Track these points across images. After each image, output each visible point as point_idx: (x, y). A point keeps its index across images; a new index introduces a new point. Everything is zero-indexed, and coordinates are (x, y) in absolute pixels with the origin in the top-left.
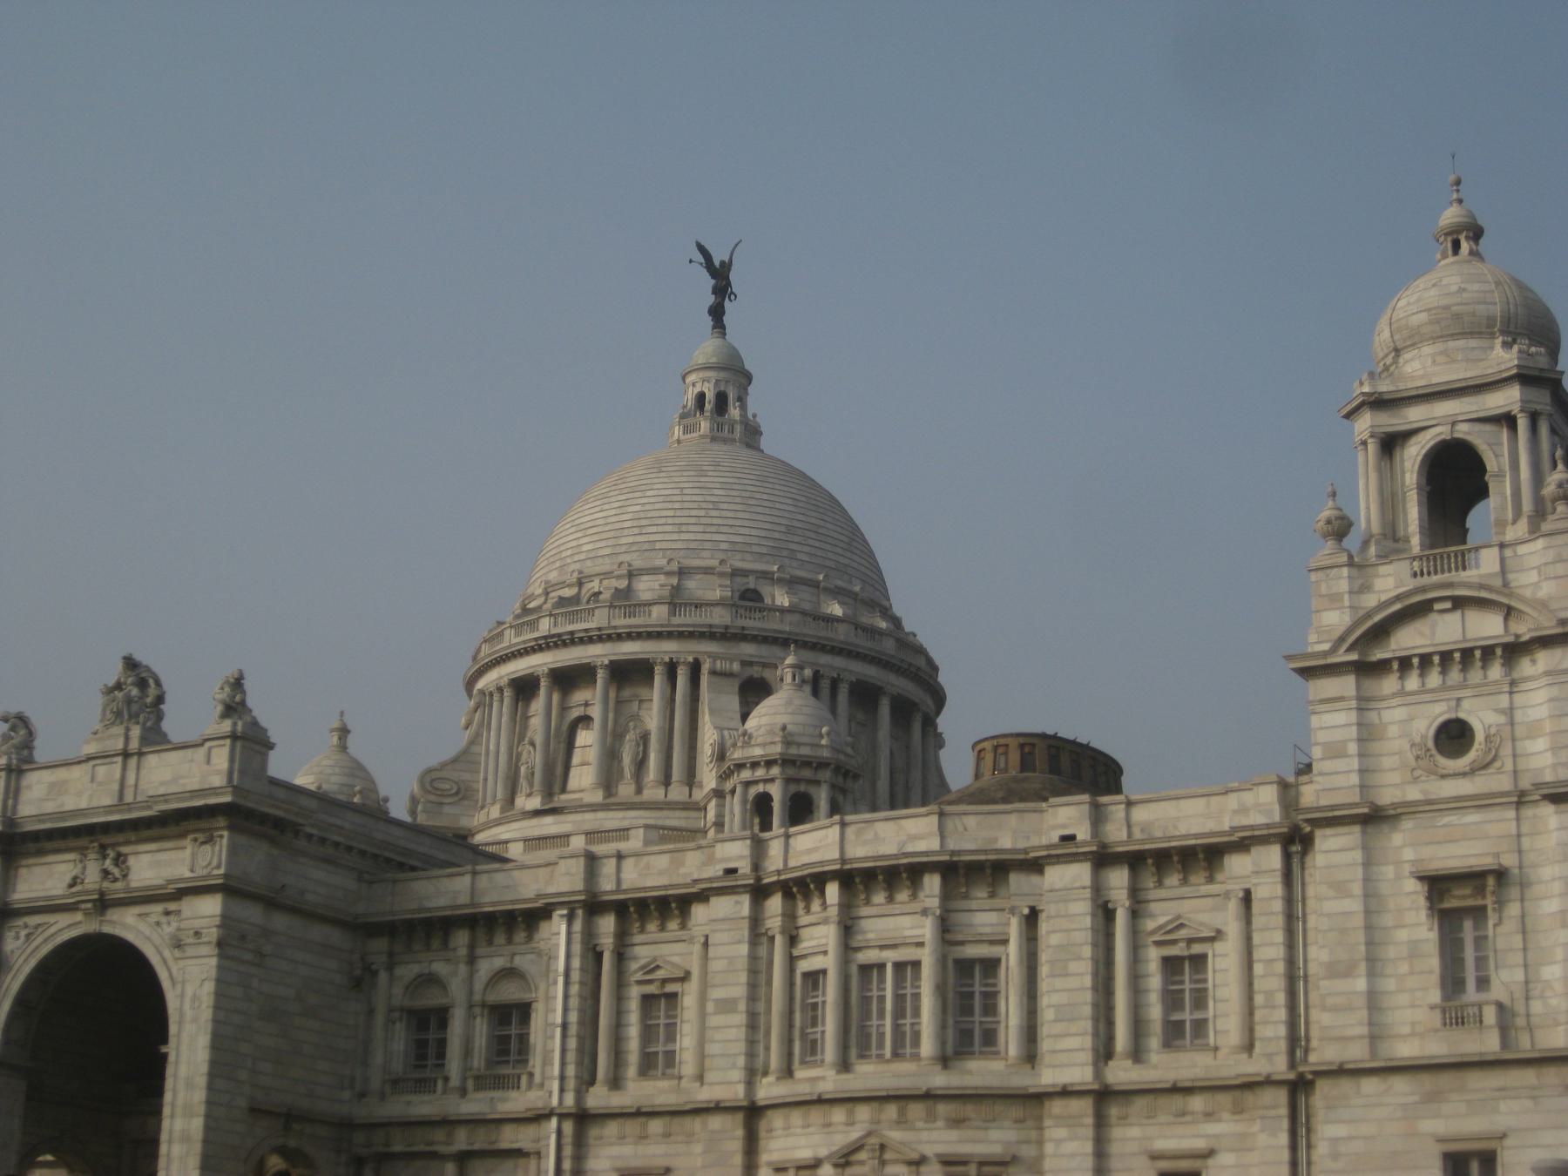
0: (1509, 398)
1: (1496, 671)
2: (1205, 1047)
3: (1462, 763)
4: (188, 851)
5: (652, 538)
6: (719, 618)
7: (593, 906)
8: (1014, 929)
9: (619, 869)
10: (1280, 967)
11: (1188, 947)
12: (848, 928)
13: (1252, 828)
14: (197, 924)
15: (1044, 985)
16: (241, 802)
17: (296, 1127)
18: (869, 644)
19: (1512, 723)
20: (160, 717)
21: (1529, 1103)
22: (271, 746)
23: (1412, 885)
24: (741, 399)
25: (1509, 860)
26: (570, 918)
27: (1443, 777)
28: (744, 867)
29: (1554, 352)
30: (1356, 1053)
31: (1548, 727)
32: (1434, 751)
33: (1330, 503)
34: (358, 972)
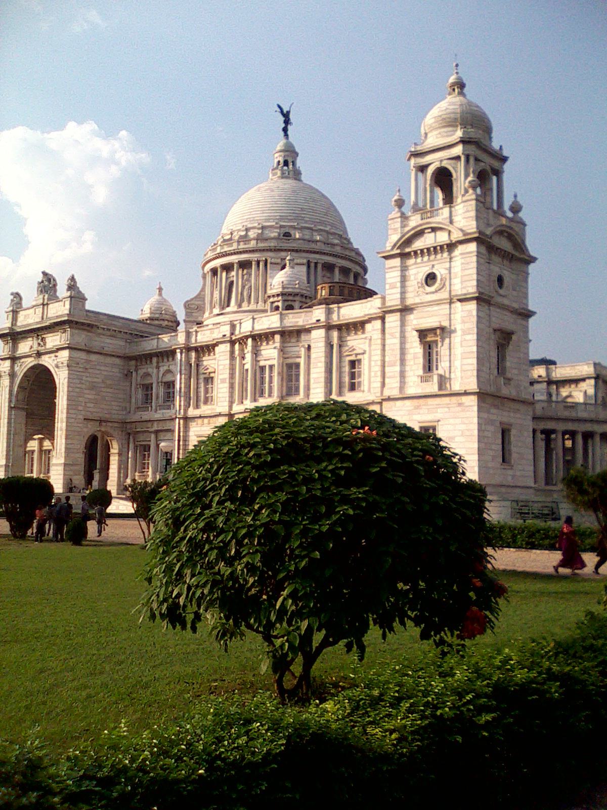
0: (458, 150)
1: (446, 255)
2: (360, 391)
3: (433, 289)
4: (59, 336)
5: (254, 216)
6: (272, 244)
7: (188, 349)
8: (303, 352)
9: (196, 336)
10: (379, 363)
11: (356, 356)
12: (256, 353)
13: (371, 315)
14: (61, 360)
15: (312, 371)
16: (71, 319)
17: (104, 424)
18: (329, 249)
19: (450, 273)
20: (55, 291)
21: (446, 409)
22: (86, 300)
23: (416, 334)
24: (294, 163)
25: (445, 324)
26: (181, 353)
27: (427, 294)
28: (228, 334)
29: (488, 130)
30: (395, 393)
31: (460, 274)
32: (425, 285)
33: (398, 194)
34: (126, 372)
